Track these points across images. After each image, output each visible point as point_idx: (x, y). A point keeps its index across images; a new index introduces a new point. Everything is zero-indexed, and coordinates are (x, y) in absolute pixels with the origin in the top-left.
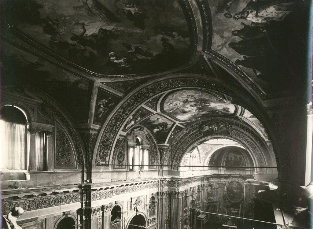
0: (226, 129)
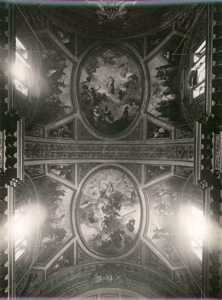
0: (123, 282)
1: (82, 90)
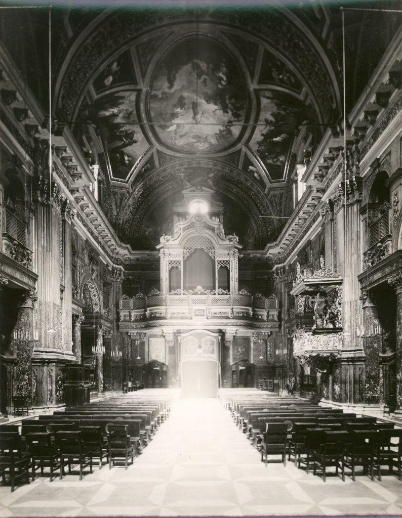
1: (242, 113)
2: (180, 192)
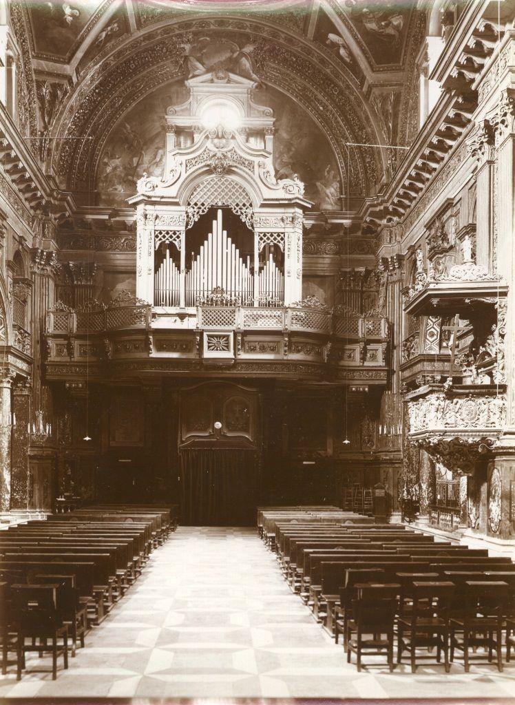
2: (181, 83)
